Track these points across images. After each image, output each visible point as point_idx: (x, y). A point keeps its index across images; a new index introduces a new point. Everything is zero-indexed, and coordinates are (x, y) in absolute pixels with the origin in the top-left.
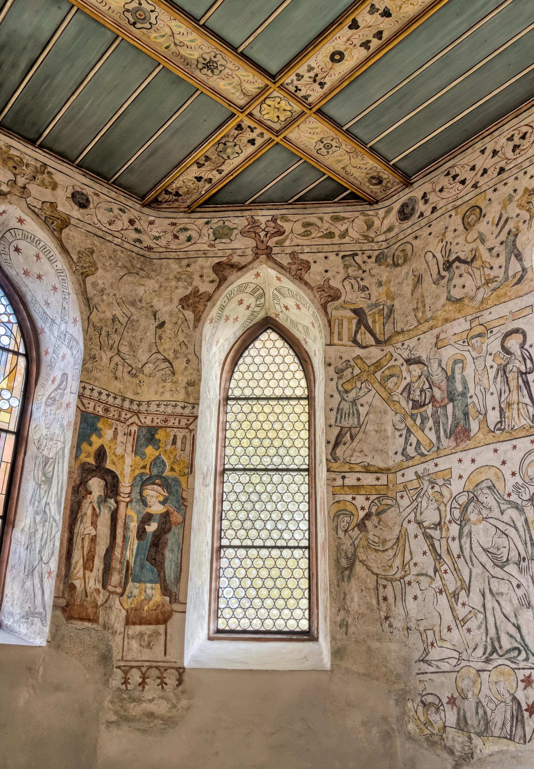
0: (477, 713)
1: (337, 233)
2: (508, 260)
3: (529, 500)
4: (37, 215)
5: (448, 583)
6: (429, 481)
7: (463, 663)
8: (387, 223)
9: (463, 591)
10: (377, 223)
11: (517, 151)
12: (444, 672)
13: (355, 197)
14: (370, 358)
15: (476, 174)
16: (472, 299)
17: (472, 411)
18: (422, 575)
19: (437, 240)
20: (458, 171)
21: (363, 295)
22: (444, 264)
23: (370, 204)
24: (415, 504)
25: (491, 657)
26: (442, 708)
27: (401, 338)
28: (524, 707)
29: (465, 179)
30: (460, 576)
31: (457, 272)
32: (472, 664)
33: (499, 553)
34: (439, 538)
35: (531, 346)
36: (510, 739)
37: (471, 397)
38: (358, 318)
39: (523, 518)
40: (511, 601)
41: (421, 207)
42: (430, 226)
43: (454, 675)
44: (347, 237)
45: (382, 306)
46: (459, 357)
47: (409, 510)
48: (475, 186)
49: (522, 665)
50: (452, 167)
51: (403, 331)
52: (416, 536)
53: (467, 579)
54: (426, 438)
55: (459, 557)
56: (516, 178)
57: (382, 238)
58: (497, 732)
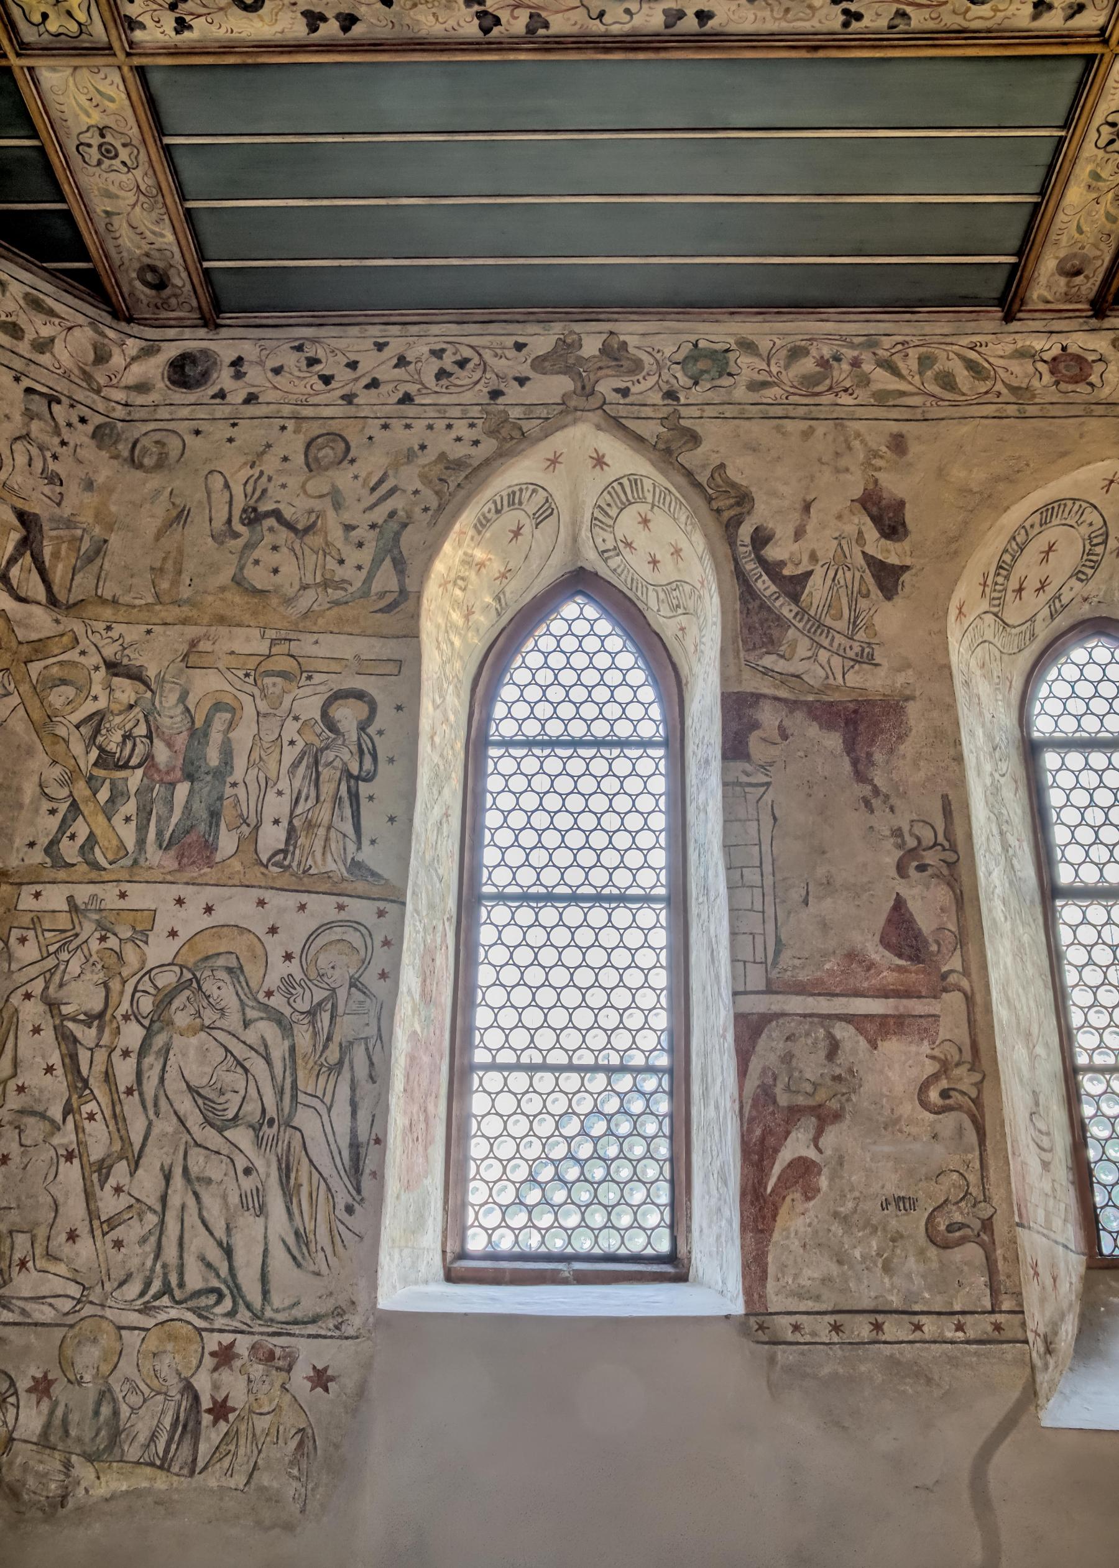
0: (97, 1413)
1: (30, 335)
2: (377, 562)
3: (308, 1012)
5: (90, 1141)
6: (98, 923)
7: (88, 1310)
8: (137, 372)
9: (124, 1163)
10: (117, 360)
11: (444, 382)
12: (36, 1324)
13: (93, 286)
14: (27, 626)
15: (356, 380)
16: (288, 601)
17: (228, 813)
18: (33, 1113)
19: (243, 459)
20: (321, 354)
21: (47, 490)
22: (244, 511)
23: (116, 314)
24: (50, 962)
25: (157, 1303)
26: (12, 1400)
27: (108, 613)
28: (206, 1403)
29: (332, 377)
30: (123, 1132)
31: (269, 539)
32: (108, 1313)
33: (222, 1100)
34: (92, 1045)
35: (380, 733)
36: (161, 1467)
37: (234, 785)
38: (24, 533)
39: (287, 1044)
40: (224, 1197)
41: (224, 378)
42: (234, 425)
43: (59, 1333)
44: (48, 354)
45: (79, 532)
46: (228, 699)
47: (33, 971)
48: (349, 399)
49: (219, 1323)
50: (314, 341)
51: (115, 602)
52: (37, 1030)
53: (137, 1139)
54: (111, 835)
55: (129, 1092)
56: (430, 427)
57: (120, 396)
58: (133, 1452)
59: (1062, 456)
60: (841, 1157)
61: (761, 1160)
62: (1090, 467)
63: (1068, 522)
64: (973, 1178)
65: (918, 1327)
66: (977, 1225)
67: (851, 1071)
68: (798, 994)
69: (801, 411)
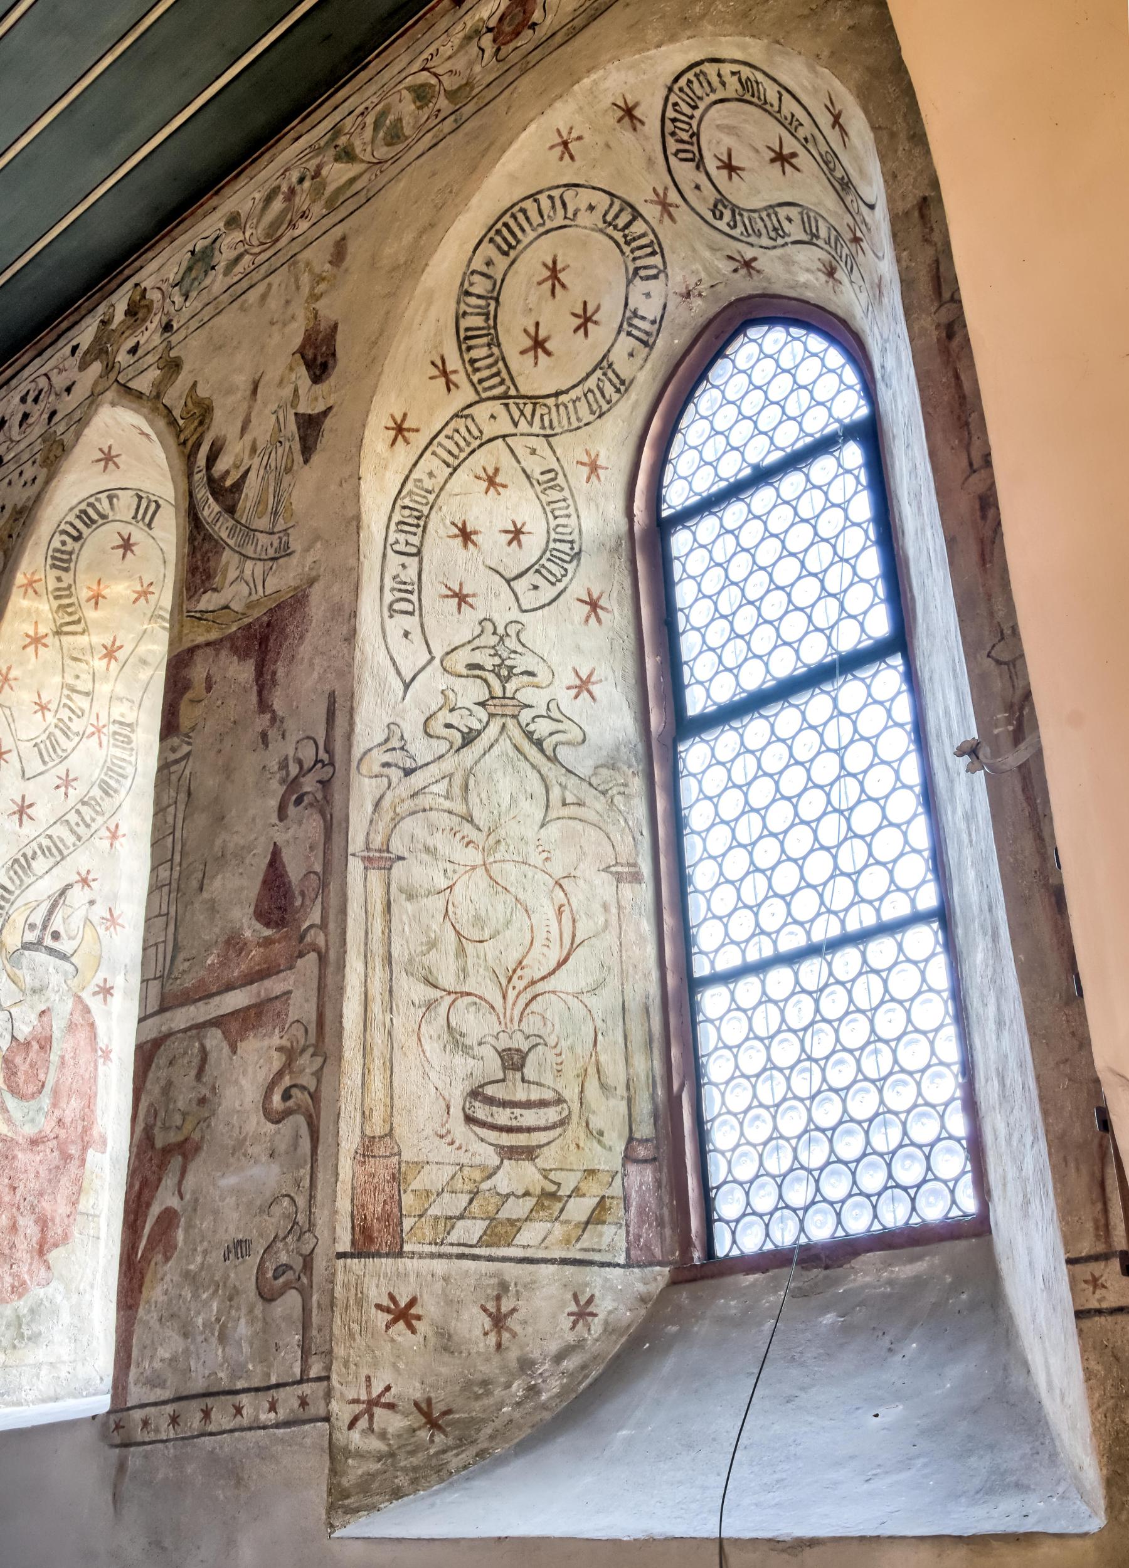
59: (490, 148)
60: (196, 1200)
61: (135, 1220)
62: (515, 146)
63: (549, 225)
64: (301, 1201)
65: (239, 1410)
66: (298, 1263)
67: (214, 1088)
68: (182, 1005)
69: (263, 269)
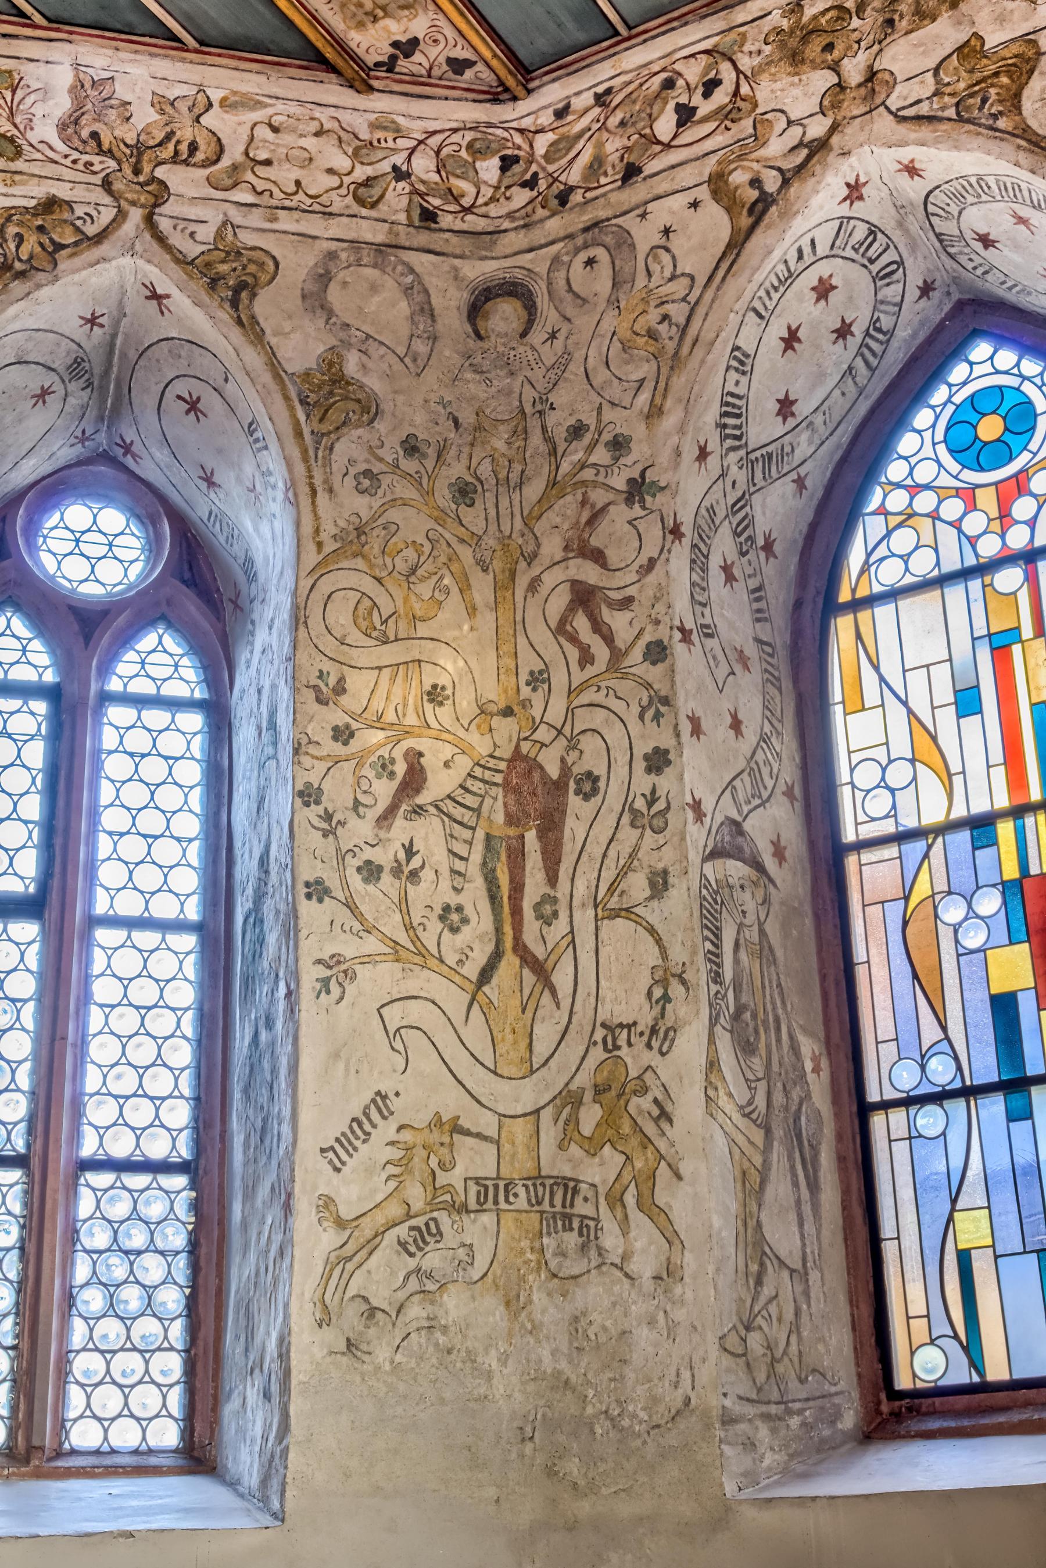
4: (930, 119)
